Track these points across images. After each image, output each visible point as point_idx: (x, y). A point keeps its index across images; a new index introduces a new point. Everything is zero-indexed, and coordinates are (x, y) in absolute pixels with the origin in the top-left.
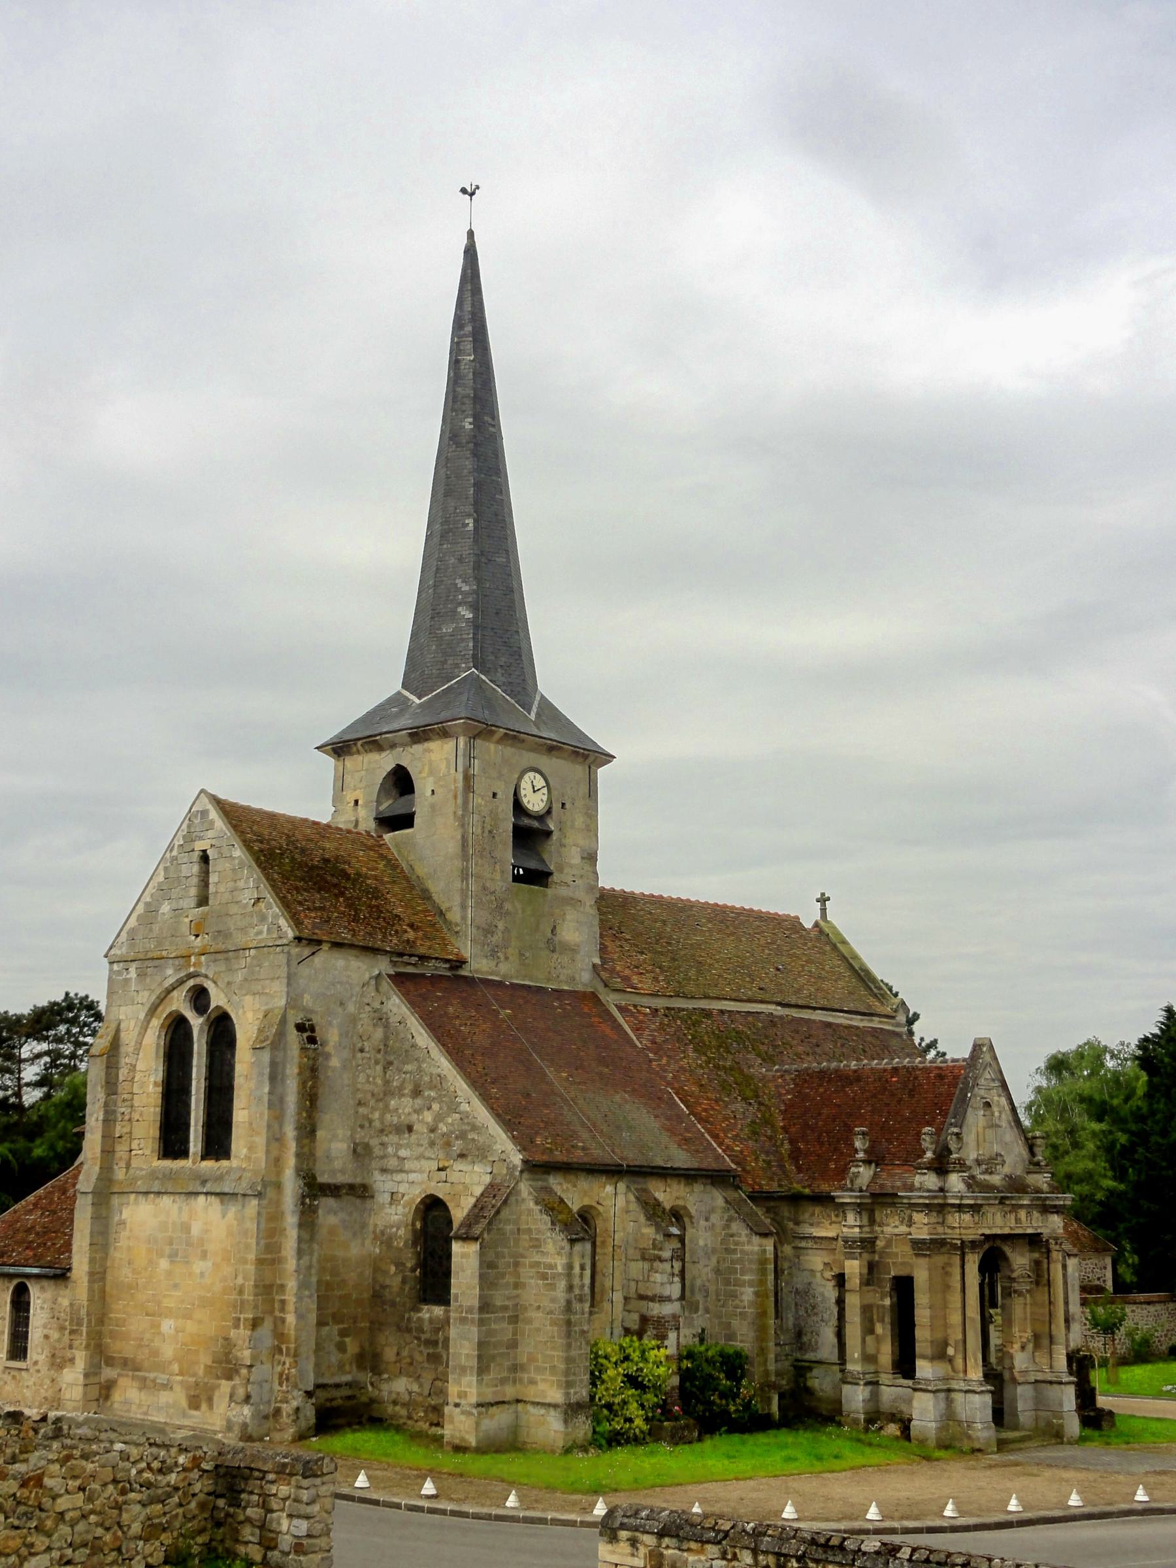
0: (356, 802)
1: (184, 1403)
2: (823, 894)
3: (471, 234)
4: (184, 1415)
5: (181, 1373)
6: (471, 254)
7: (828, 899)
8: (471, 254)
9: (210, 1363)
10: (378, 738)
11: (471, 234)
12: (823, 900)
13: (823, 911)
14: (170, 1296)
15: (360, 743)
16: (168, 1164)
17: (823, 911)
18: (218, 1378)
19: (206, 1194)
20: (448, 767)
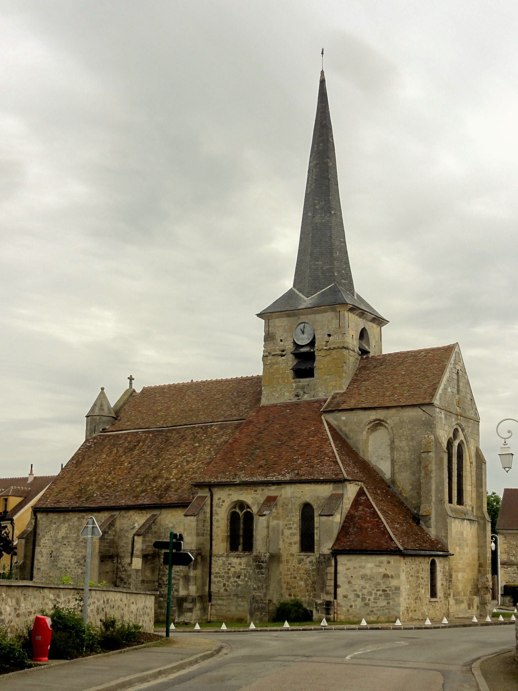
0: (353, 335)
1: (467, 608)
2: (131, 376)
3: (322, 72)
4: (467, 613)
5: (464, 596)
6: (323, 82)
7: (133, 379)
8: (323, 82)
9: (471, 590)
10: (366, 313)
11: (322, 72)
12: (131, 379)
13: (131, 384)
14: (459, 563)
15: (360, 311)
16: (458, 506)
17: (131, 384)
18: (473, 595)
19: (466, 519)
20: (378, 338)
